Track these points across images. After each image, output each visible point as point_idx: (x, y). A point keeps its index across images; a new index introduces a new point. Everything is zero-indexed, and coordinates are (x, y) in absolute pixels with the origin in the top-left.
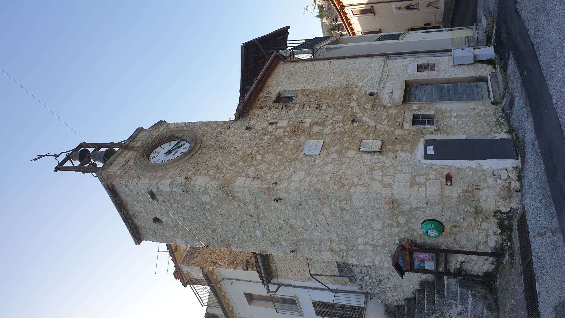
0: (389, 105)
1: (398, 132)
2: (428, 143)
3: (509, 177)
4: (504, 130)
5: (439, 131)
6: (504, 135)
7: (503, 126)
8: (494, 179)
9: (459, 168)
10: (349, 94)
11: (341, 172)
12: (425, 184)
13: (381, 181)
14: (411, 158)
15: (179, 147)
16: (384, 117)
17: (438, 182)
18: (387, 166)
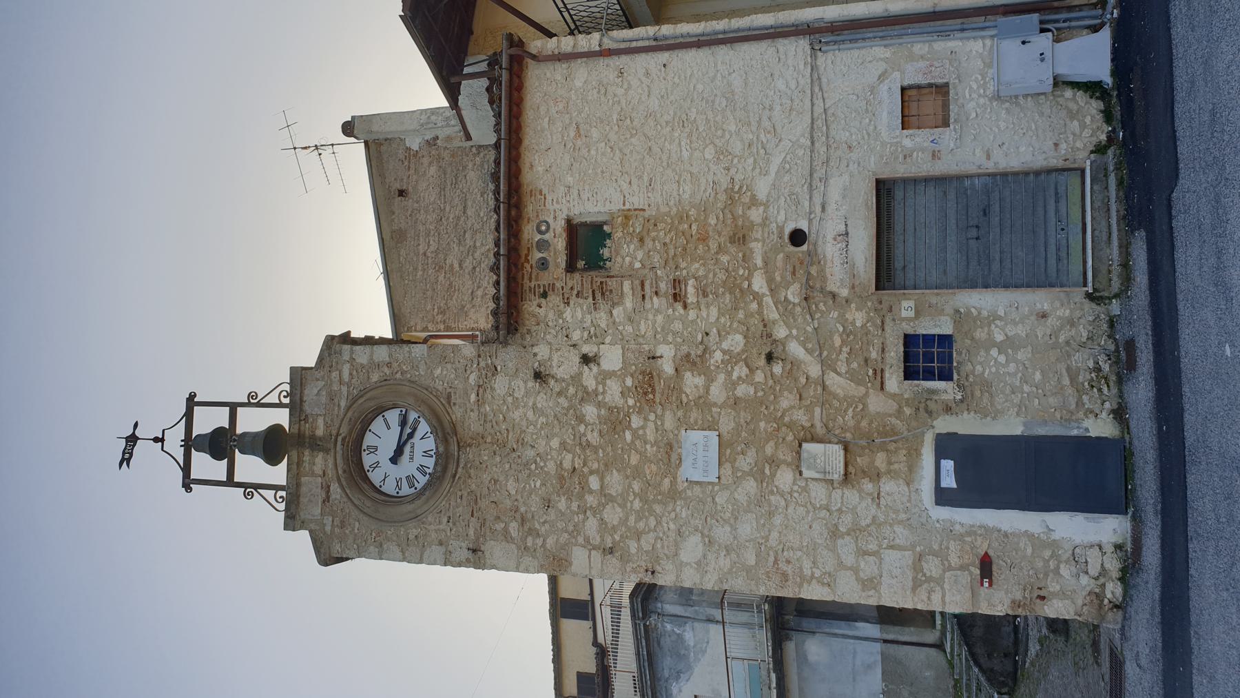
0: (844, 292)
1: (876, 403)
2: (946, 446)
3: (1103, 572)
4: (1107, 405)
5: (965, 403)
6: (1101, 427)
8: (1073, 568)
9: (1006, 535)
10: (740, 238)
11: (773, 542)
12: (940, 581)
13: (856, 570)
14: (909, 501)
15: (411, 436)
17: (965, 578)
18: (863, 524)
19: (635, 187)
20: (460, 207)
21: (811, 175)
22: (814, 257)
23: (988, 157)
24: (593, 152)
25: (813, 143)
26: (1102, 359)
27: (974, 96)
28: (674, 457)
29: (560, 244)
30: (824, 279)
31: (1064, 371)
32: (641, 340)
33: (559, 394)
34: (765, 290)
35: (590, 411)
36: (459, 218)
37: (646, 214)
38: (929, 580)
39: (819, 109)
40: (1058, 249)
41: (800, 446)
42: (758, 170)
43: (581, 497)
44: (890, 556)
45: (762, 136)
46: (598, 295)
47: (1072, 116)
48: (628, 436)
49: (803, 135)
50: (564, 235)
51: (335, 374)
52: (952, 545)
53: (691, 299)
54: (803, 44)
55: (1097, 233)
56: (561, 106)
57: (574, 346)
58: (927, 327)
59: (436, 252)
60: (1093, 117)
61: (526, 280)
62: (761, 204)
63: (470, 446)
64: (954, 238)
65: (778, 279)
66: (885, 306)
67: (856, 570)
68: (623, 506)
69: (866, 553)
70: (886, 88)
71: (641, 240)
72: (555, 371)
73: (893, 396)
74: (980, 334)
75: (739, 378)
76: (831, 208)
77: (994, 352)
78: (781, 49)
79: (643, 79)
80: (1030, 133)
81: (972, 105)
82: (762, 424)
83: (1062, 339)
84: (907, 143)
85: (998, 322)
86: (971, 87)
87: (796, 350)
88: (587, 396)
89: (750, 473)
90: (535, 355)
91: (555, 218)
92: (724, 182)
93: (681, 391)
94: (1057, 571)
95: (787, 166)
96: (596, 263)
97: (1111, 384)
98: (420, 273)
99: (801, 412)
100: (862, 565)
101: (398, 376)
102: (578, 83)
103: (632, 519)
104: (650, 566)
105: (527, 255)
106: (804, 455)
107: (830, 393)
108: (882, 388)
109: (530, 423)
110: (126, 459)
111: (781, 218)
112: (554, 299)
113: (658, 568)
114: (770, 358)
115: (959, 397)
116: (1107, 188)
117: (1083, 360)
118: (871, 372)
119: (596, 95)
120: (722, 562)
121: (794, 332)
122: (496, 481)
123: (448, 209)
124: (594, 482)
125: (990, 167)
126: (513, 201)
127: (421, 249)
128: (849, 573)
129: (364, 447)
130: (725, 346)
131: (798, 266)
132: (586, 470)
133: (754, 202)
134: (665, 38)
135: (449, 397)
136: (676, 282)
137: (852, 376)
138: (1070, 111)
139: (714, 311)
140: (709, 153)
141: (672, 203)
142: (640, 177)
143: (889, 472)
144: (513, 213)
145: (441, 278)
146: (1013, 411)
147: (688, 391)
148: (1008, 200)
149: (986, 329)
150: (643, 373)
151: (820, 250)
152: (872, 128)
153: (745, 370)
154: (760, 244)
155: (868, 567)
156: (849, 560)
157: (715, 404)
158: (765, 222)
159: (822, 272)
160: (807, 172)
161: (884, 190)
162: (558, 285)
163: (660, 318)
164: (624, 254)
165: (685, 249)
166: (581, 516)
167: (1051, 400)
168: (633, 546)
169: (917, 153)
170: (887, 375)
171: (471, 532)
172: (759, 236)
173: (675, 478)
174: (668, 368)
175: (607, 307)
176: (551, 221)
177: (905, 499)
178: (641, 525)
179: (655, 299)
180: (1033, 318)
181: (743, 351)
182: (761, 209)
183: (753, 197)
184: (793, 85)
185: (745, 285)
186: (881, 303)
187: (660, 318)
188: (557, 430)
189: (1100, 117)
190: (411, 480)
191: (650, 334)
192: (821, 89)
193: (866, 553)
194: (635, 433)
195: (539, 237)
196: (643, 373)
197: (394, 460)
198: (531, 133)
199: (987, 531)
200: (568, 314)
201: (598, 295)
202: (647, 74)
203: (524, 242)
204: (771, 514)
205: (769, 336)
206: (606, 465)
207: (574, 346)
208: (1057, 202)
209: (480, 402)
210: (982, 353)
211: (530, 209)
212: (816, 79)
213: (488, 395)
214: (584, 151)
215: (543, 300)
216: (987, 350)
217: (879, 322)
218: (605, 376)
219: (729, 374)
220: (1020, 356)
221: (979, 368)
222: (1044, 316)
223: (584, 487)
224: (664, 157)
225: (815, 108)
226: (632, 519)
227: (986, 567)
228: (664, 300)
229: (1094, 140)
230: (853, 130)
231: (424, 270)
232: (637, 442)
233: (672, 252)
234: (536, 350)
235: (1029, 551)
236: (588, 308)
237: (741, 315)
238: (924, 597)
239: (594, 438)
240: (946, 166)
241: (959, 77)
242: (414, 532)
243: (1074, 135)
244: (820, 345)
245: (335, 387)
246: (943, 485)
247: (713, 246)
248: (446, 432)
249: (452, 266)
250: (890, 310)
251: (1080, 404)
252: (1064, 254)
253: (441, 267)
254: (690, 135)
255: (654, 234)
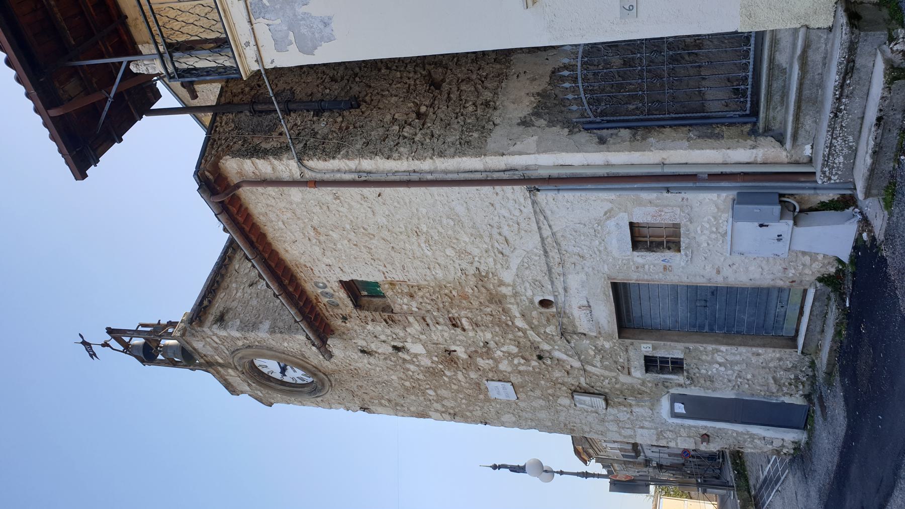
1: (623, 378)
7: (801, 387)
16: (592, 353)
23: (718, 272)
25: (546, 252)
27: (705, 232)
31: (770, 378)
45: (496, 245)
62: (509, 285)
81: (703, 238)
84: (640, 260)
86: (702, 226)
87: (557, 354)
92: (471, 270)
121: (556, 347)
154: (515, 306)
158: (516, 295)
160: (545, 268)
162: (353, 315)
169: (648, 267)
181: (519, 352)
195: (319, 291)
223: (424, 394)
225: (543, 232)
229: (823, 270)
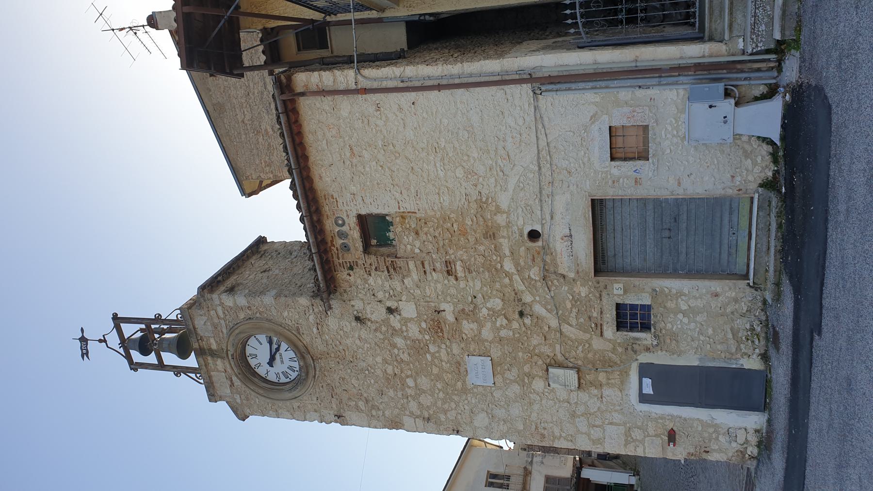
0: (572, 275)
1: (597, 344)
2: (645, 370)
3: (747, 441)
4: (757, 351)
5: (660, 345)
6: (753, 363)
7: (757, 342)
8: (727, 438)
9: (685, 419)
10: (491, 234)
11: (534, 415)
12: (642, 442)
13: (588, 435)
14: (622, 400)
15: (278, 349)
16: (569, 306)
17: (658, 441)
18: (592, 411)
19: (405, 196)
20: (261, 84)
21: (541, 192)
22: (546, 249)
23: (679, 184)
24: (367, 169)
25: (540, 168)
26: (756, 323)
27: (669, 136)
28: (462, 370)
29: (356, 234)
30: (556, 265)
31: (729, 330)
32: (428, 299)
33: (376, 330)
34: (513, 270)
35: (399, 341)
36: (262, 93)
37: (418, 215)
38: (634, 441)
39: (543, 143)
40: (729, 247)
41: (547, 370)
42: (499, 188)
43: (403, 390)
44: (610, 429)
45: (499, 161)
46: (392, 270)
47: (747, 155)
48: (429, 357)
49: (532, 163)
50: (358, 228)
51: (212, 313)
52: (650, 424)
53: (460, 274)
54: (527, 88)
55: (759, 245)
56: (334, 132)
57: (380, 301)
58: (631, 299)
59: (252, 119)
60: (763, 157)
61: (335, 259)
62: (504, 212)
63: (321, 359)
64: (652, 236)
65: (523, 264)
66: (602, 284)
67: (588, 435)
68: (432, 396)
69: (594, 426)
70: (597, 128)
71: (417, 233)
72: (369, 316)
73: (610, 341)
74: (670, 305)
75: (502, 325)
76: (558, 217)
77: (680, 316)
78: (508, 91)
79: (398, 113)
80: (713, 167)
81: (667, 143)
82: (520, 354)
83: (729, 310)
84: (615, 172)
85: (683, 297)
86: (666, 129)
87: (539, 309)
88: (395, 332)
89: (515, 381)
90: (353, 306)
91: (348, 216)
92: (474, 196)
93: (461, 332)
94: (717, 439)
95: (521, 185)
96: (385, 242)
97: (761, 339)
98: (243, 136)
99: (546, 347)
100: (592, 432)
101: (258, 315)
102: (345, 113)
103: (439, 403)
104: (455, 428)
105: (332, 241)
106: (551, 375)
107: (566, 336)
108: (602, 335)
109: (359, 347)
110: (85, 354)
111: (520, 222)
112: (359, 271)
113: (460, 429)
114: (521, 314)
115: (655, 343)
116: (769, 215)
117: (743, 324)
118: (593, 325)
119: (361, 125)
120: (501, 427)
121: (537, 298)
122: (343, 379)
123: (251, 85)
124: (410, 382)
125: (680, 193)
126: (313, 209)
127: (240, 117)
128: (584, 436)
129: (247, 354)
130: (488, 305)
131: (536, 256)
132: (403, 375)
133: (498, 210)
134: (410, 79)
135: (298, 329)
136: (447, 263)
137: (580, 327)
138: (745, 151)
139: (478, 284)
140: (460, 173)
141: (436, 208)
142: (408, 189)
143: (608, 384)
144: (315, 218)
145: (260, 140)
146: (692, 352)
147: (467, 332)
148: (693, 211)
149: (675, 302)
150: (433, 320)
151: (551, 246)
152: (586, 160)
153: (505, 322)
154: (506, 241)
155: (596, 433)
156: (584, 429)
157: (487, 341)
158: (509, 225)
159: (554, 260)
160: (537, 190)
161: (598, 206)
162: (360, 262)
163: (439, 286)
164: (405, 242)
165: (451, 241)
166: (405, 401)
167: (719, 347)
168: (443, 417)
169: (623, 181)
170: (605, 328)
171: (334, 406)
172: (505, 234)
173: (464, 381)
174: (451, 318)
175: (400, 278)
176: (345, 218)
177: (619, 399)
178: (446, 406)
179: (433, 273)
180: (709, 296)
181: (503, 309)
182: (505, 216)
183: (498, 207)
184: (521, 122)
185: (499, 266)
186: (598, 283)
187: (439, 286)
188: (378, 351)
189: (768, 158)
190: (285, 374)
191: (433, 295)
192: (544, 127)
193: (594, 426)
194: (433, 355)
195: (337, 229)
196: (433, 320)
197: (271, 363)
198: (314, 151)
199: (672, 418)
200: (371, 280)
201: (392, 270)
202: (400, 109)
203: (328, 232)
204: (531, 404)
205: (520, 300)
206: (416, 373)
207: (380, 301)
208: (731, 213)
209: (321, 334)
210: (672, 316)
211: (326, 209)
212: (539, 118)
213: (325, 329)
214: (360, 168)
215: (351, 272)
216: (676, 314)
217: (598, 295)
218: (406, 321)
219: (494, 323)
220: (698, 319)
221: (669, 326)
222: (717, 295)
223: (404, 384)
224: (425, 175)
225: (540, 142)
226: (439, 403)
227: (672, 437)
228: (440, 275)
229: (763, 175)
230: (571, 160)
231: (246, 134)
232: (436, 360)
233: (441, 244)
234: (352, 303)
235: (700, 428)
236: (386, 278)
237: (498, 286)
238: (632, 449)
239: (405, 357)
240: (647, 191)
241: (657, 121)
242: (298, 404)
243: (747, 170)
244: (556, 307)
245: (216, 321)
246: (644, 392)
247: (472, 240)
248: (302, 353)
249: (266, 130)
250: (606, 287)
251: (738, 349)
252: (734, 251)
253: (258, 132)
254: (442, 159)
255: (426, 229)
